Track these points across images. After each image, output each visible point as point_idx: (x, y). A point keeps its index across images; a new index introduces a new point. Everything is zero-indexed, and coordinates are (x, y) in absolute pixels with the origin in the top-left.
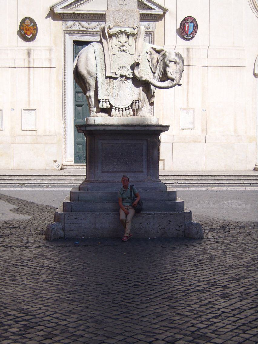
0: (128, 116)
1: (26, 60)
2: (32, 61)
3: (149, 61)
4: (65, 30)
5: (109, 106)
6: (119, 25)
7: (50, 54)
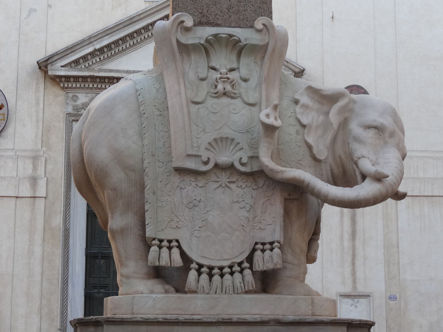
4: (69, 114)
5: (177, 260)
6: (211, 19)
7: (35, 168)
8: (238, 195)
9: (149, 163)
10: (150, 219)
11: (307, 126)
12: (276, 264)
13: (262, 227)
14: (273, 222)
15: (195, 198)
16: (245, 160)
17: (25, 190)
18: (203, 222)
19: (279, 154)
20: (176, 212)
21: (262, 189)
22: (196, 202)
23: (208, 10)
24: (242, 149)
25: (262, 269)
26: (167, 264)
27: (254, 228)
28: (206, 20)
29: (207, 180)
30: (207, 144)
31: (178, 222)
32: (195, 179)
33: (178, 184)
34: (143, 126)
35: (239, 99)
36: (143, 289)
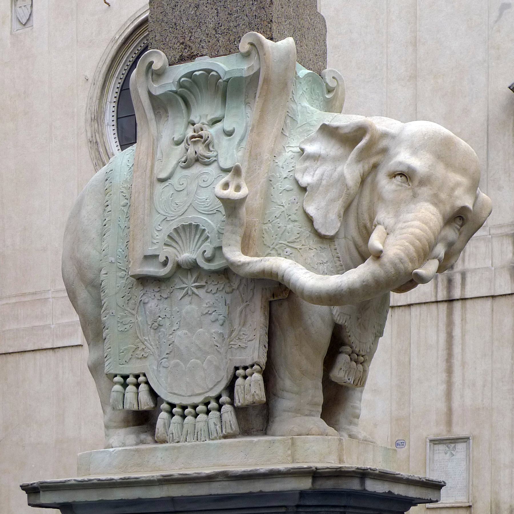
8: (208, 304)
10: (108, 350)
12: (253, 395)
13: (243, 345)
14: (254, 336)
15: (159, 315)
19: (263, 237)
20: (141, 336)
21: (238, 291)
22: (160, 320)
25: (242, 402)
26: (132, 407)
27: (231, 347)
29: (172, 287)
30: (166, 238)
31: (144, 349)
32: (159, 288)
33: (141, 298)
36: (113, 442)
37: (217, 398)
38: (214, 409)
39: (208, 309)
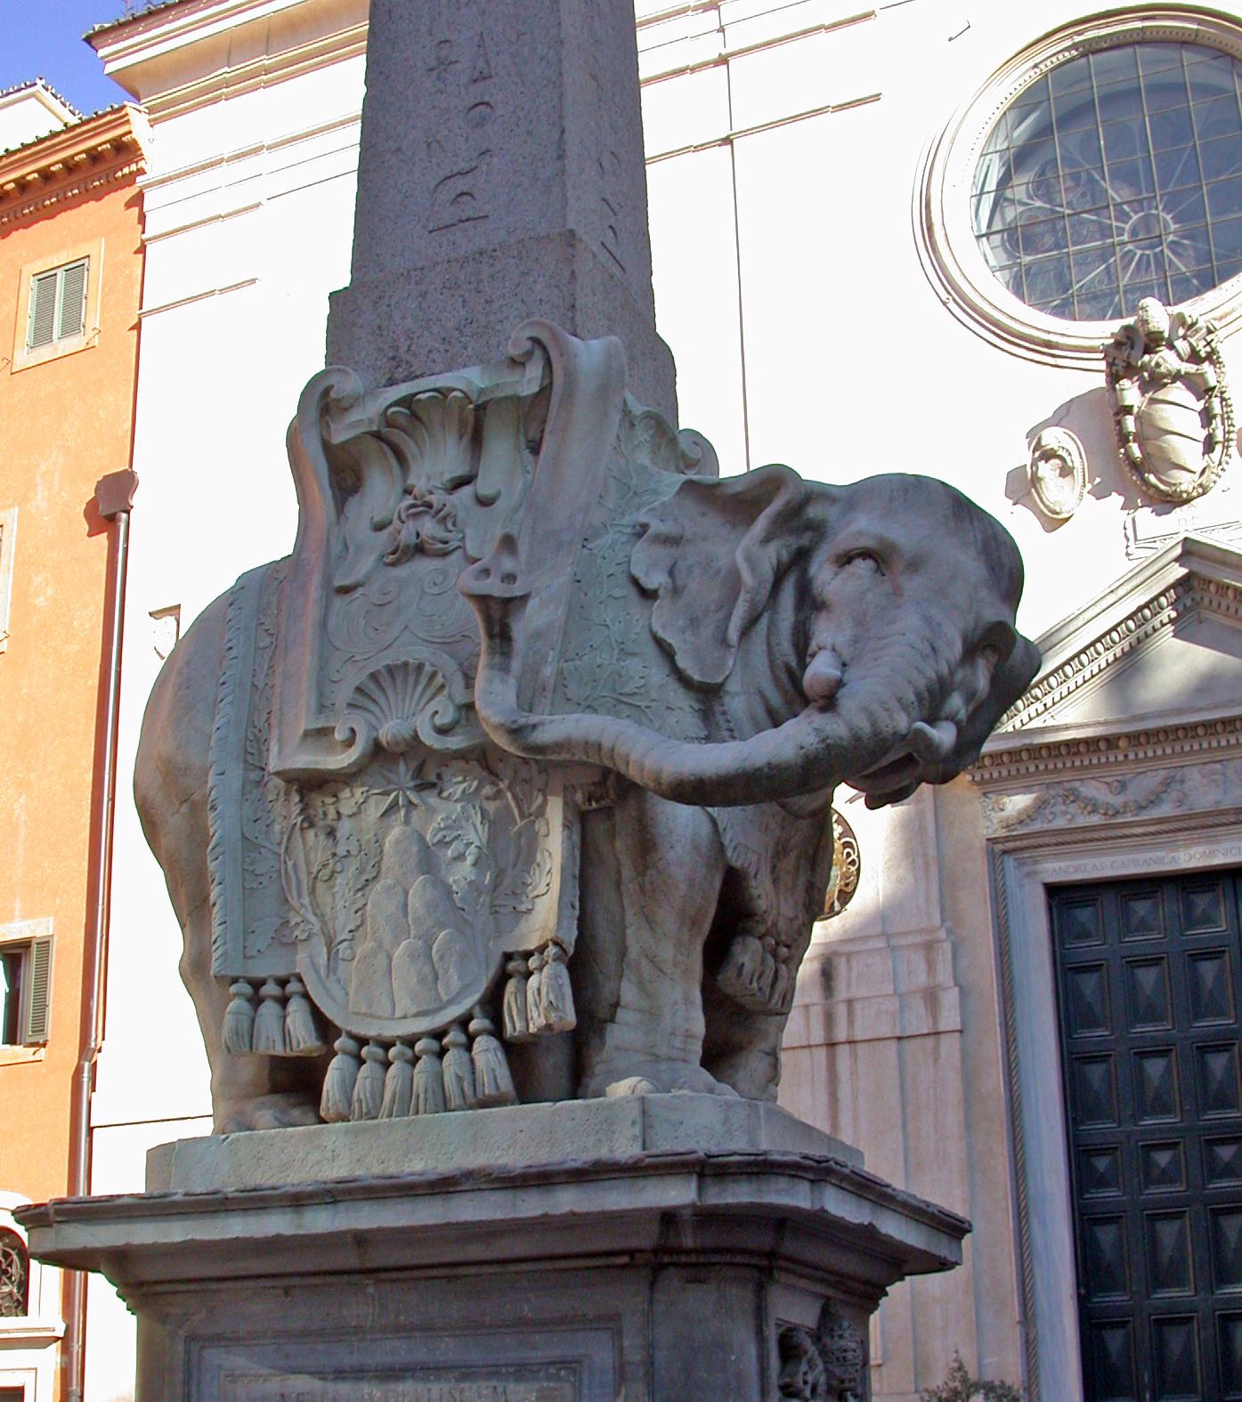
0: (455, 1100)
1: (812, 1008)
2: (841, 1011)
3: (648, 595)
7: (931, 968)
9: (222, 774)
11: (661, 592)
16: (445, 719)
17: (918, 1021)
18: (360, 913)
23: (409, 347)
24: (442, 687)
27: (496, 912)
28: (406, 373)
34: (221, 681)
35: (458, 554)
37: (464, 1022)
38: (457, 1045)
39: (444, 833)
